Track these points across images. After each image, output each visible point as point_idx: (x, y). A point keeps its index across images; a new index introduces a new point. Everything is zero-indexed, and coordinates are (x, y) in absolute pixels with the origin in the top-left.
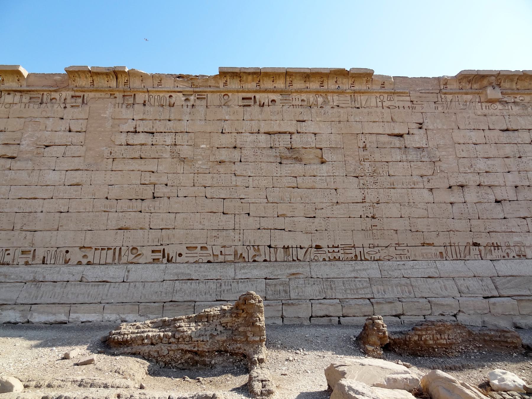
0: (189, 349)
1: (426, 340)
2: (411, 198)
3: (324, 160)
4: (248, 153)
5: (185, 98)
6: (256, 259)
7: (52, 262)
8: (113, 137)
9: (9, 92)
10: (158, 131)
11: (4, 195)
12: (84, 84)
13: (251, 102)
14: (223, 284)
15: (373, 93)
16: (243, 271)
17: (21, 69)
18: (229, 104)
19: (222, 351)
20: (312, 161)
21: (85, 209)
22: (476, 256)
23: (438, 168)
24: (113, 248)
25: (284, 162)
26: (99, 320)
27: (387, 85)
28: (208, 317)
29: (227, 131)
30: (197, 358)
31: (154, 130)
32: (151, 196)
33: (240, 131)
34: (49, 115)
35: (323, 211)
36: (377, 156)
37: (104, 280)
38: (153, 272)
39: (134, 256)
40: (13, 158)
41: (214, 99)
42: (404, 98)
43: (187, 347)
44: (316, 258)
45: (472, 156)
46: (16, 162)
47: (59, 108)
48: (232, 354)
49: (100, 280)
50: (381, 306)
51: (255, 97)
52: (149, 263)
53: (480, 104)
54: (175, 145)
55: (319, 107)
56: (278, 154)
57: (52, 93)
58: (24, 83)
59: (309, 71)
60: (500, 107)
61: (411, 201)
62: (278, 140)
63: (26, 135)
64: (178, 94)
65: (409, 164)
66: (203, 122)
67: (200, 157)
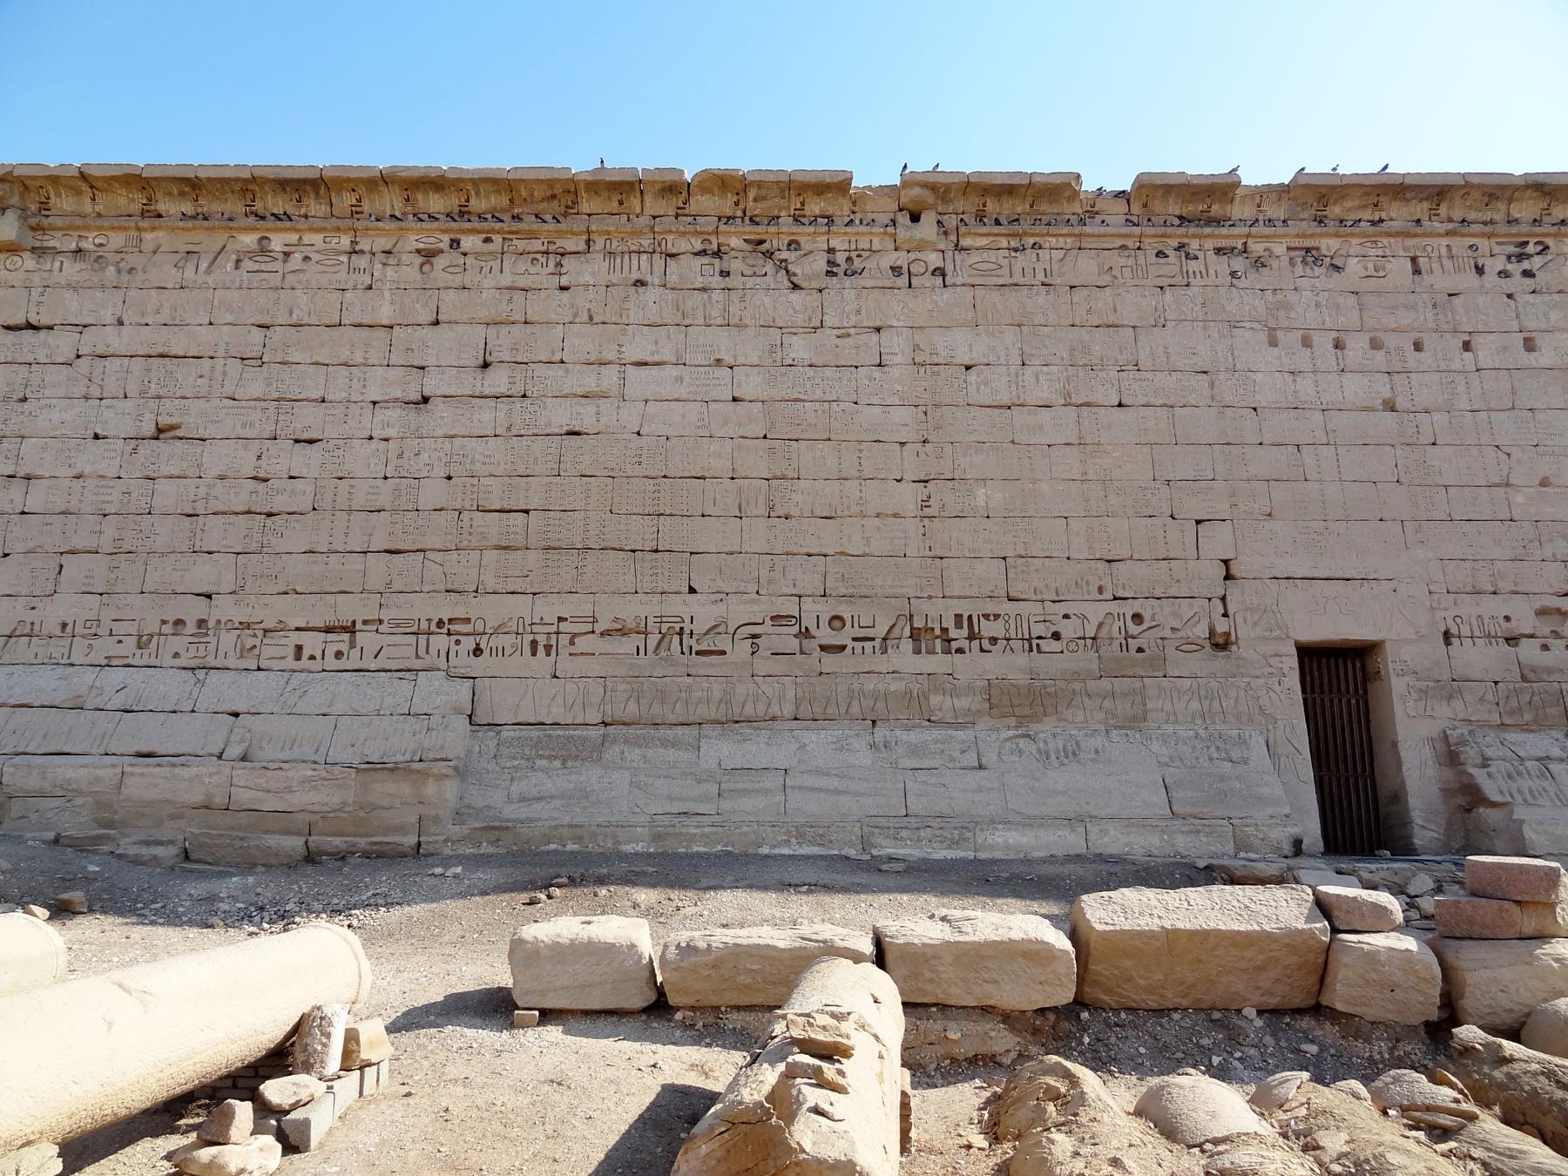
60: (29, 262)
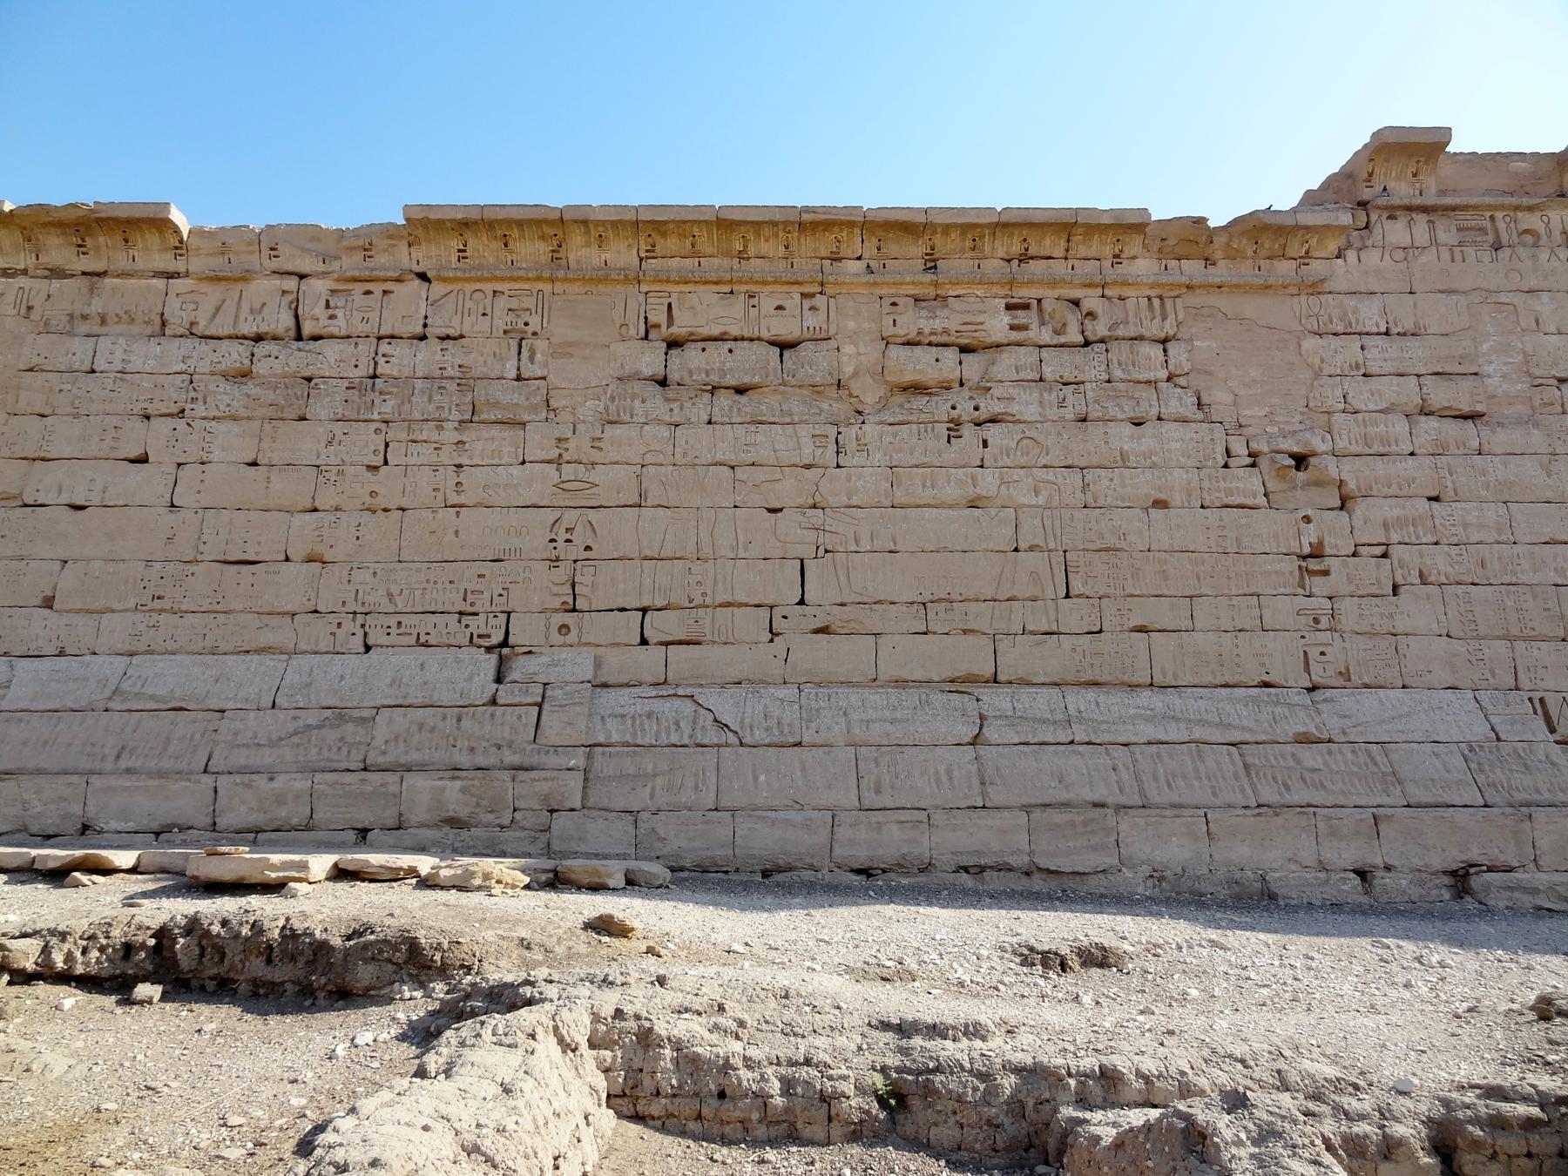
9: (1392, 213)
11: (1499, 531)
34: (1533, 283)
46: (1493, 432)
57: (1520, 215)
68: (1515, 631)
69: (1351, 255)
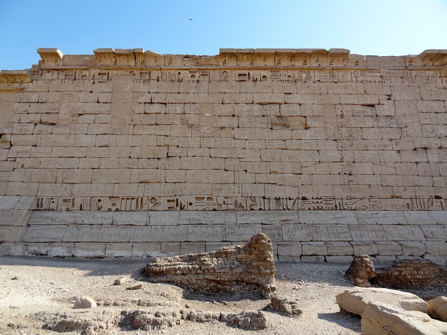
0: (213, 279)
1: (405, 275)
2: (382, 158)
3: (308, 126)
4: (244, 120)
5: (191, 75)
6: (253, 208)
7: (88, 209)
8: (133, 107)
9: (48, 71)
10: (170, 102)
11: (48, 154)
12: (108, 63)
13: (246, 78)
14: (227, 228)
15: (348, 69)
16: (243, 218)
17: (59, 51)
18: (228, 79)
19: (239, 281)
20: (298, 127)
21: (113, 166)
22: (438, 207)
23: (405, 133)
24: (136, 198)
25: (274, 127)
26: (129, 256)
27: (360, 63)
28: (226, 253)
29: (226, 102)
30: (220, 286)
31: (166, 102)
32: (166, 155)
33: (238, 102)
35: (307, 168)
36: (353, 123)
37: (130, 223)
38: (170, 218)
39: (153, 204)
40: (54, 124)
41: (215, 75)
42: (375, 73)
43: (212, 278)
44: (303, 207)
45: (434, 122)
46: (56, 128)
47: (89, 84)
48: (247, 284)
49: (128, 224)
50: (360, 247)
51: (249, 73)
52: (166, 210)
53: (440, 79)
54: (184, 113)
55: (303, 81)
56: (269, 121)
57: (83, 71)
58: (60, 63)
59: (295, 52)
61: (382, 161)
62: (269, 109)
63: (63, 106)
64: (186, 71)
65: (380, 130)
66: (207, 95)
67: (205, 124)
68: (42, 181)
69: (35, 82)
